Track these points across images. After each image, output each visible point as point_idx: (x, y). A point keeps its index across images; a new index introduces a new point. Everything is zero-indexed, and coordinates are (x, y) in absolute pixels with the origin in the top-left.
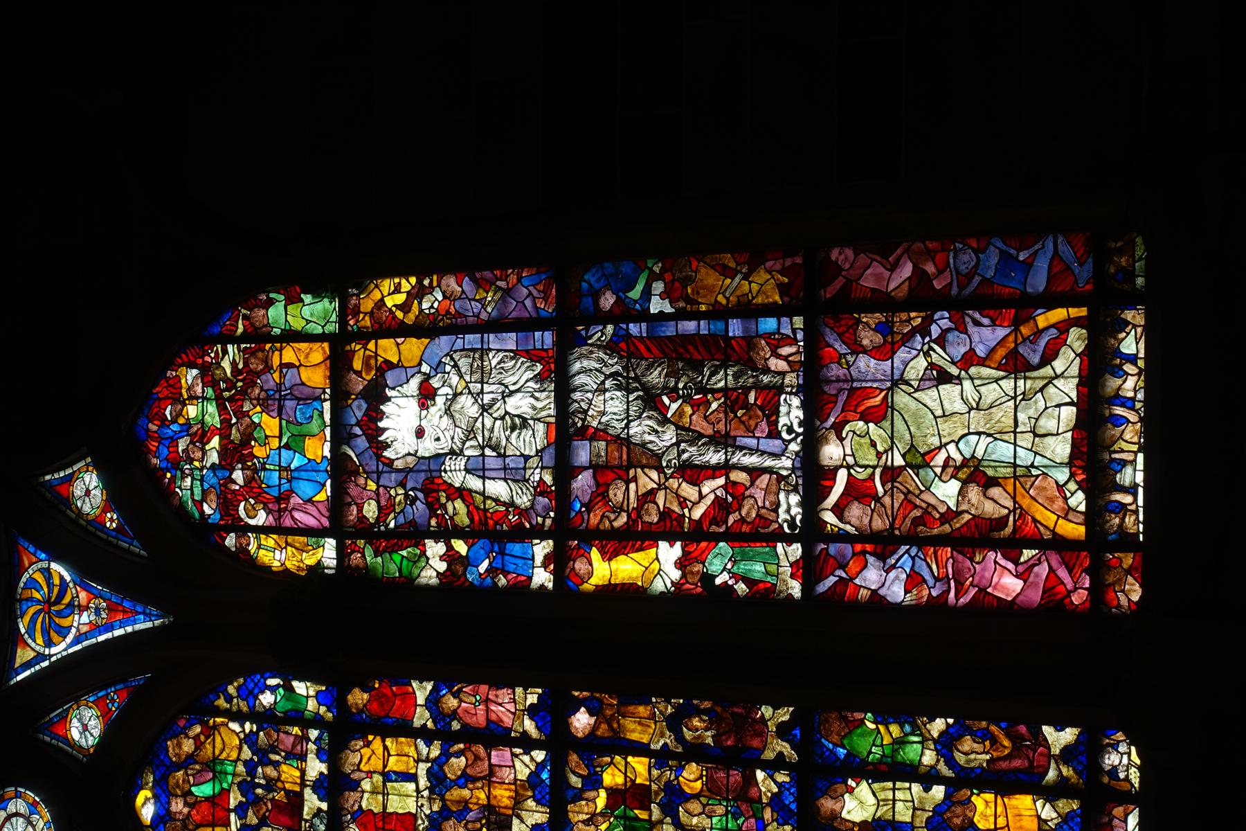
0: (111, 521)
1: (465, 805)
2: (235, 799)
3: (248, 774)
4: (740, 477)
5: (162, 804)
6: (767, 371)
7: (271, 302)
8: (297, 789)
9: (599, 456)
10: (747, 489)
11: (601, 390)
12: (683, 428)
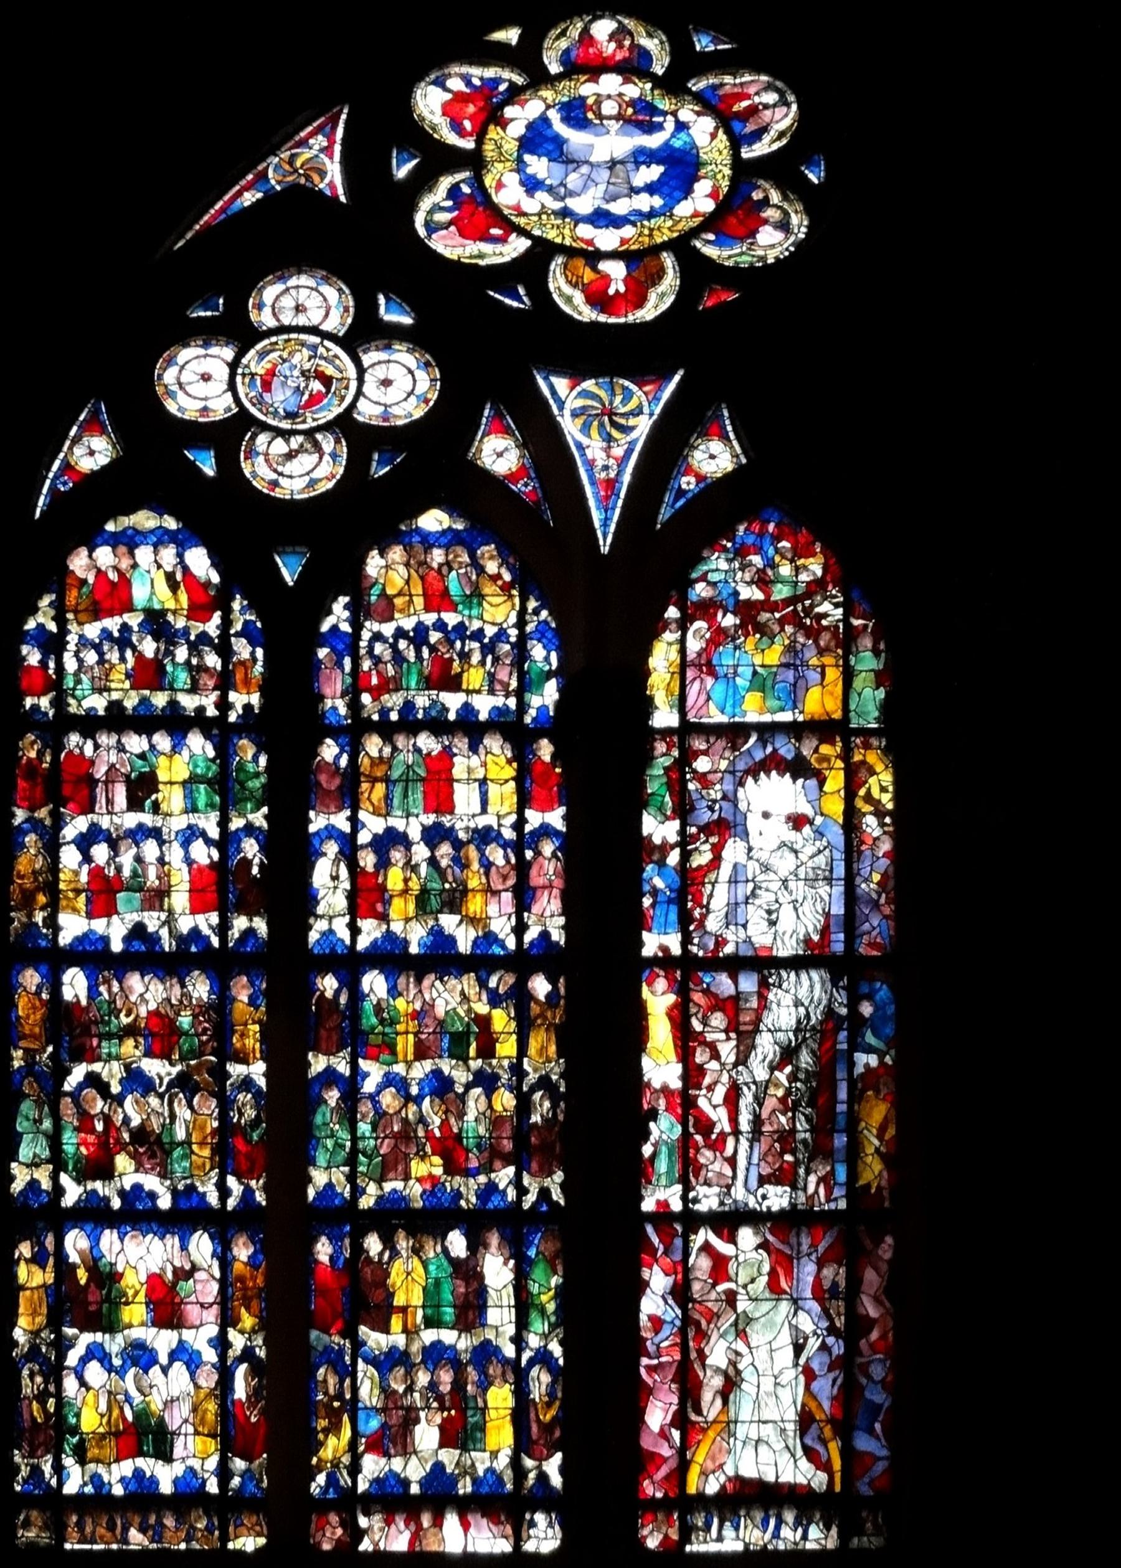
0: (688, 483)
1: (465, 866)
2: (451, 619)
3: (472, 632)
4: (729, 1151)
5: (438, 539)
6: (808, 1172)
7: (876, 652)
8: (464, 686)
9: (747, 1001)
10: (721, 1153)
11: (797, 1003)
12: (766, 1088)
